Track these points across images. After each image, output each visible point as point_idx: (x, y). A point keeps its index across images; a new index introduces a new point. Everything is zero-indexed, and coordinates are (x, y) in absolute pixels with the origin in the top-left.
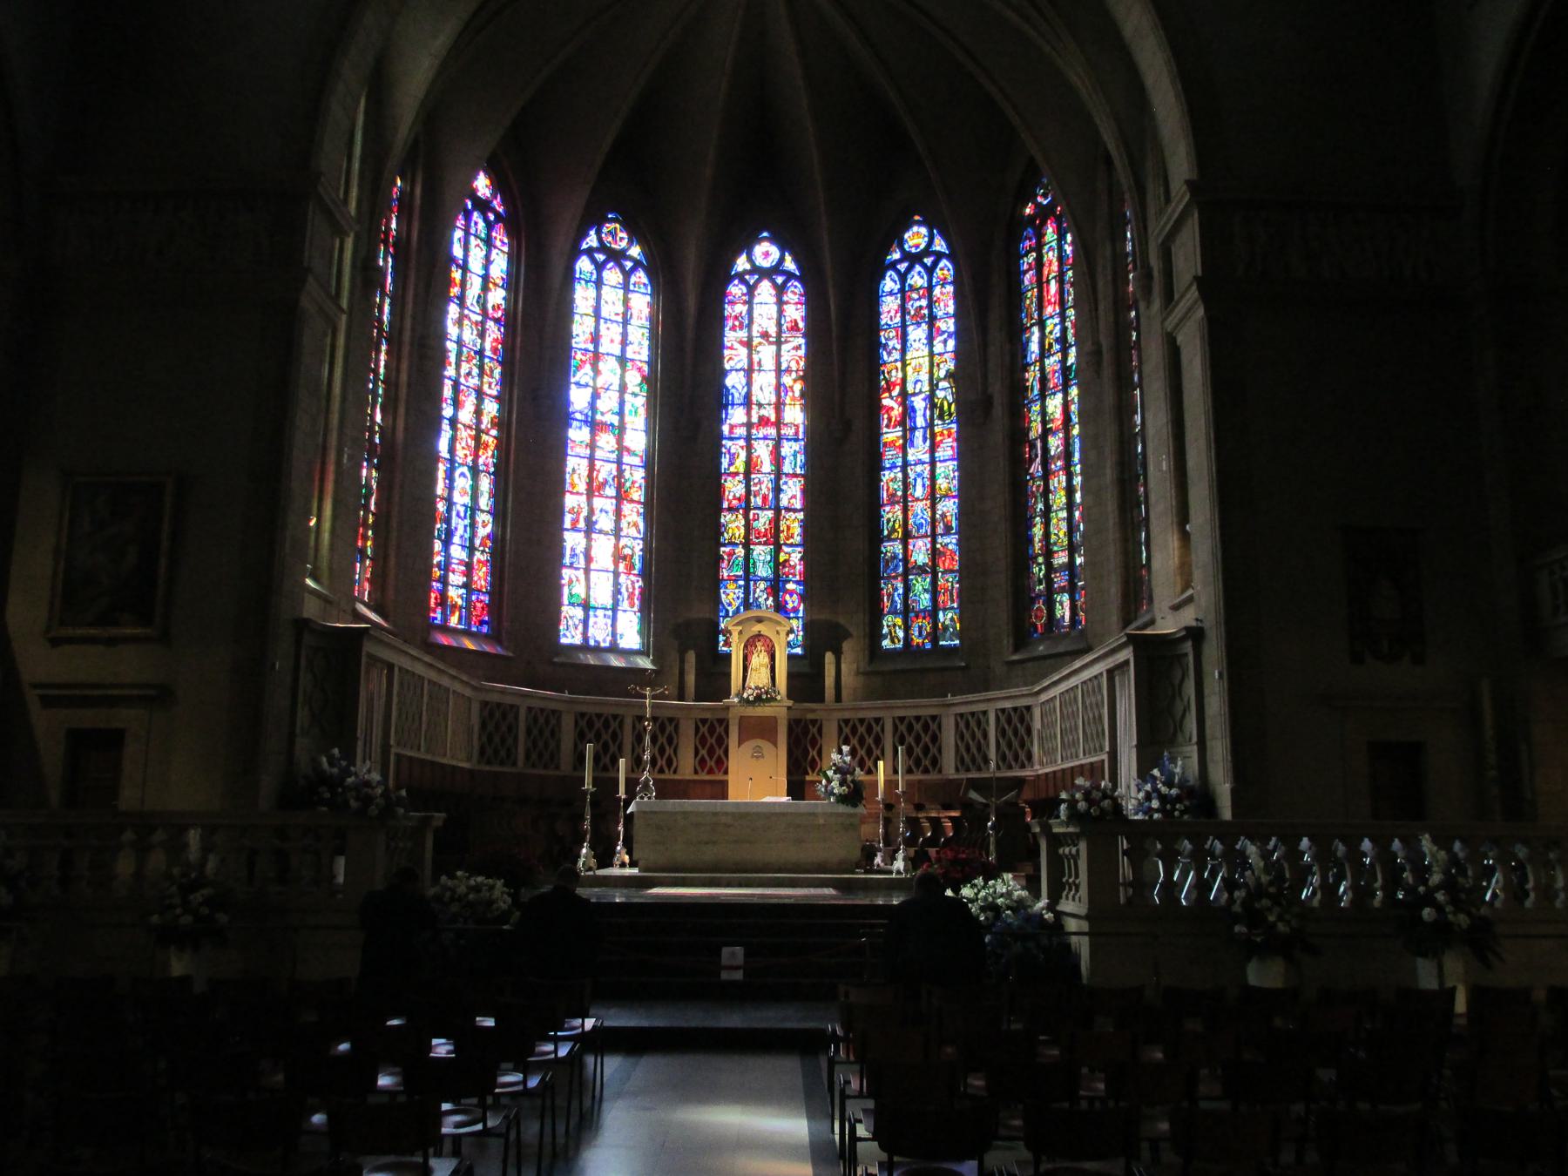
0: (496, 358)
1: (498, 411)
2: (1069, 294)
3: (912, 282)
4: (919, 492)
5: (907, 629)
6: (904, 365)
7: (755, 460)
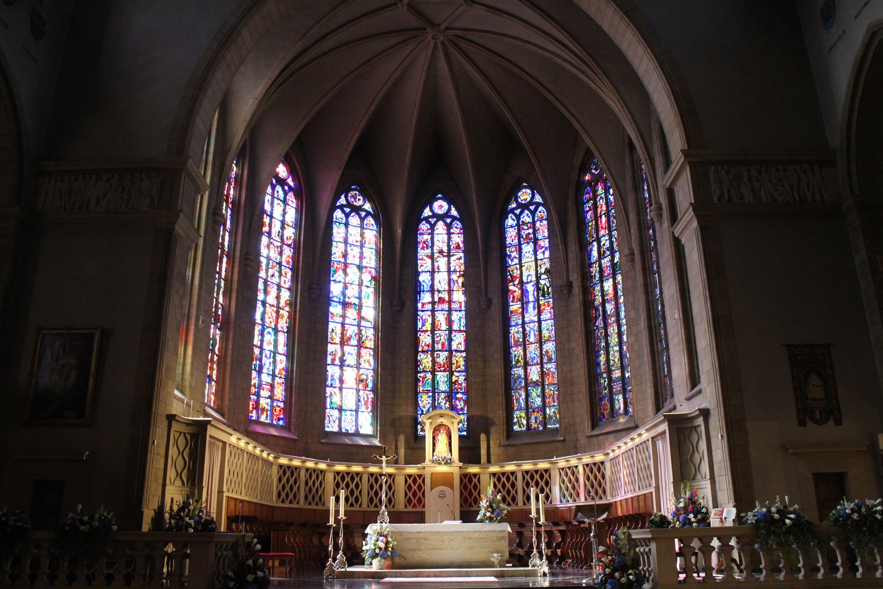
0: (288, 266)
1: (290, 297)
2: (613, 223)
3: (523, 220)
4: (532, 339)
5: (528, 419)
6: (521, 266)
7: (437, 323)
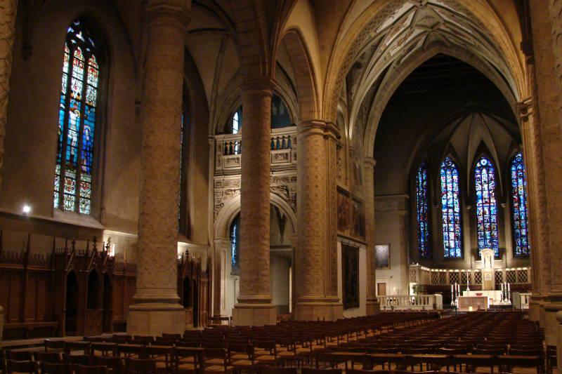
4: (523, 218)
5: (521, 249)
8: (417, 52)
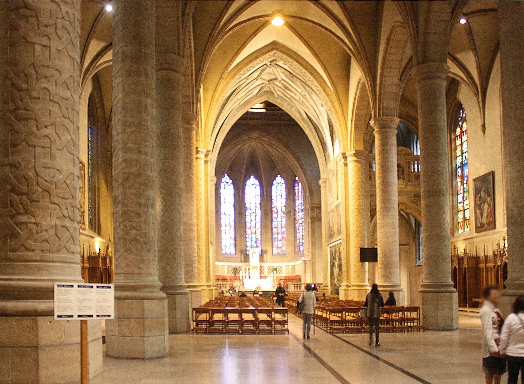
8: (253, 97)
